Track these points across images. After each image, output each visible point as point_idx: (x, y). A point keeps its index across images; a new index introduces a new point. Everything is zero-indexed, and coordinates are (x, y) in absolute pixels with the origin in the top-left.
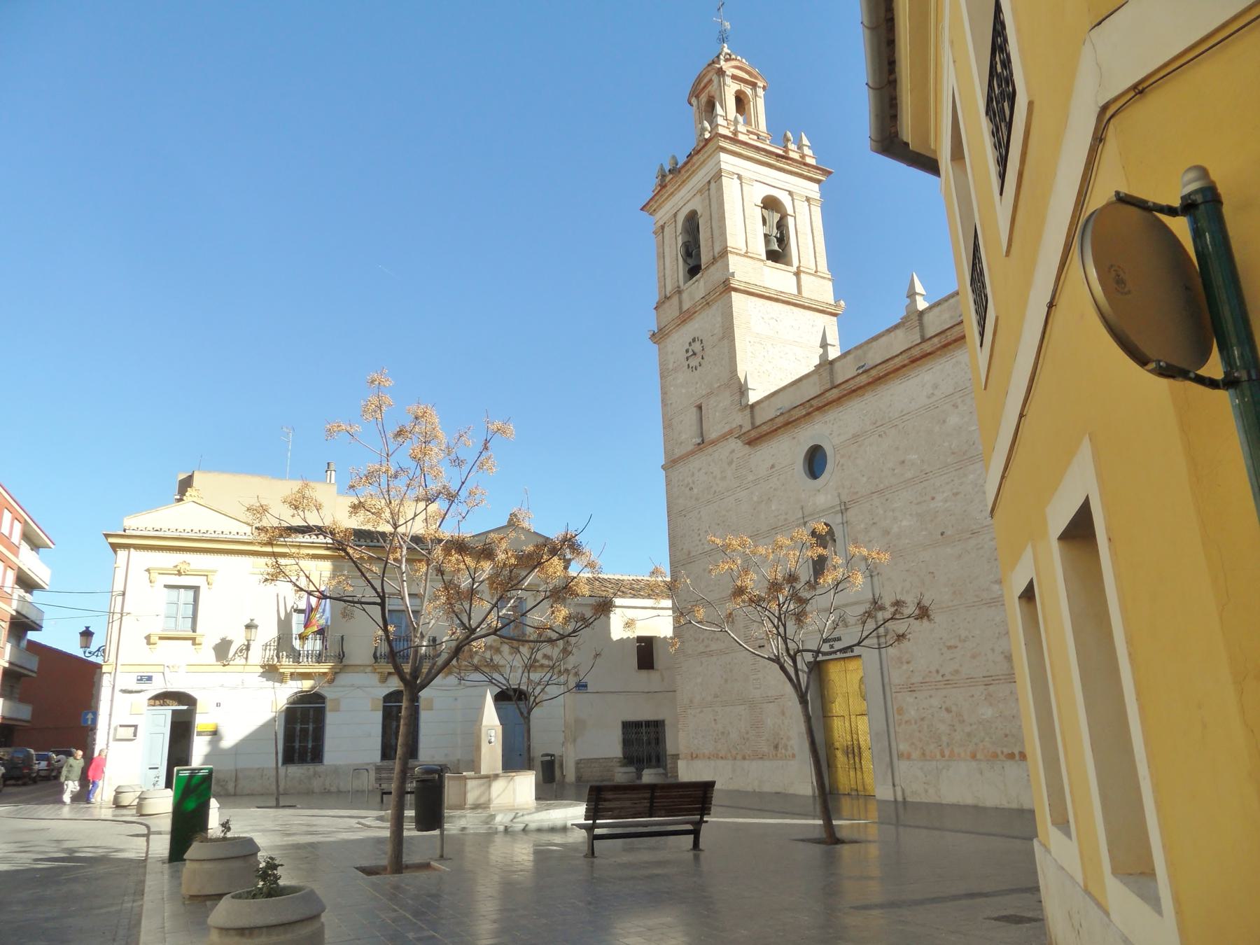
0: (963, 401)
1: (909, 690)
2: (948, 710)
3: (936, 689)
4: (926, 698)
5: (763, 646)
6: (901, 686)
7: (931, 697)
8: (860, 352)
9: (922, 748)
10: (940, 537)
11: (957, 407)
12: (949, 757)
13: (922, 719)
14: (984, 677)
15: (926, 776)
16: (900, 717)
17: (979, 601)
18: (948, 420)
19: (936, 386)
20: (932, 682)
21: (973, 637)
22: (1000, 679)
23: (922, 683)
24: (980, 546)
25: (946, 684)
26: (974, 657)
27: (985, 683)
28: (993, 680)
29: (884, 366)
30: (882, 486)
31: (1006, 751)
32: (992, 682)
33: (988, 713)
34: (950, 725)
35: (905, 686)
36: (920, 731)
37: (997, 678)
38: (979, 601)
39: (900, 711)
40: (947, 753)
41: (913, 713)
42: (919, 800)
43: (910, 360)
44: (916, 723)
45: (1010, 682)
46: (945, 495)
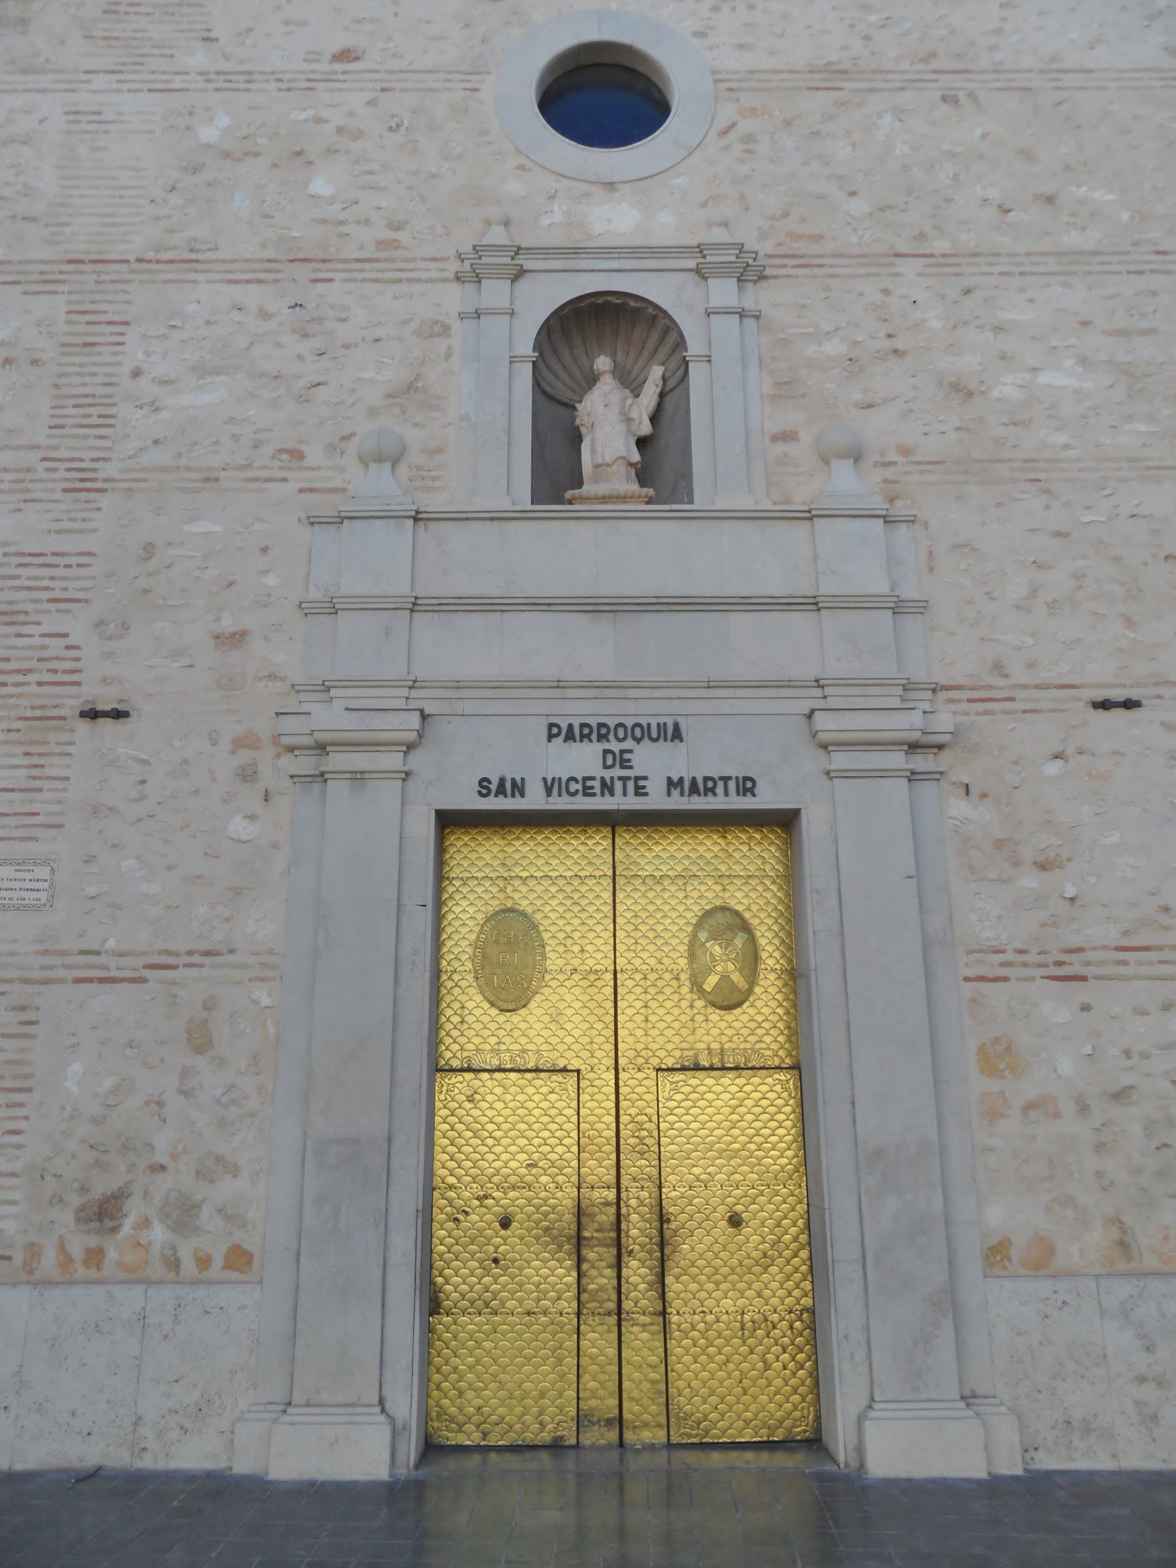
5: (118, 715)
6: (1009, 956)
9: (1116, 1221)
13: (1121, 1095)
16: (994, 1085)
30: (942, 245)
35: (1032, 957)
41: (1066, 1067)
42: (1102, 1463)
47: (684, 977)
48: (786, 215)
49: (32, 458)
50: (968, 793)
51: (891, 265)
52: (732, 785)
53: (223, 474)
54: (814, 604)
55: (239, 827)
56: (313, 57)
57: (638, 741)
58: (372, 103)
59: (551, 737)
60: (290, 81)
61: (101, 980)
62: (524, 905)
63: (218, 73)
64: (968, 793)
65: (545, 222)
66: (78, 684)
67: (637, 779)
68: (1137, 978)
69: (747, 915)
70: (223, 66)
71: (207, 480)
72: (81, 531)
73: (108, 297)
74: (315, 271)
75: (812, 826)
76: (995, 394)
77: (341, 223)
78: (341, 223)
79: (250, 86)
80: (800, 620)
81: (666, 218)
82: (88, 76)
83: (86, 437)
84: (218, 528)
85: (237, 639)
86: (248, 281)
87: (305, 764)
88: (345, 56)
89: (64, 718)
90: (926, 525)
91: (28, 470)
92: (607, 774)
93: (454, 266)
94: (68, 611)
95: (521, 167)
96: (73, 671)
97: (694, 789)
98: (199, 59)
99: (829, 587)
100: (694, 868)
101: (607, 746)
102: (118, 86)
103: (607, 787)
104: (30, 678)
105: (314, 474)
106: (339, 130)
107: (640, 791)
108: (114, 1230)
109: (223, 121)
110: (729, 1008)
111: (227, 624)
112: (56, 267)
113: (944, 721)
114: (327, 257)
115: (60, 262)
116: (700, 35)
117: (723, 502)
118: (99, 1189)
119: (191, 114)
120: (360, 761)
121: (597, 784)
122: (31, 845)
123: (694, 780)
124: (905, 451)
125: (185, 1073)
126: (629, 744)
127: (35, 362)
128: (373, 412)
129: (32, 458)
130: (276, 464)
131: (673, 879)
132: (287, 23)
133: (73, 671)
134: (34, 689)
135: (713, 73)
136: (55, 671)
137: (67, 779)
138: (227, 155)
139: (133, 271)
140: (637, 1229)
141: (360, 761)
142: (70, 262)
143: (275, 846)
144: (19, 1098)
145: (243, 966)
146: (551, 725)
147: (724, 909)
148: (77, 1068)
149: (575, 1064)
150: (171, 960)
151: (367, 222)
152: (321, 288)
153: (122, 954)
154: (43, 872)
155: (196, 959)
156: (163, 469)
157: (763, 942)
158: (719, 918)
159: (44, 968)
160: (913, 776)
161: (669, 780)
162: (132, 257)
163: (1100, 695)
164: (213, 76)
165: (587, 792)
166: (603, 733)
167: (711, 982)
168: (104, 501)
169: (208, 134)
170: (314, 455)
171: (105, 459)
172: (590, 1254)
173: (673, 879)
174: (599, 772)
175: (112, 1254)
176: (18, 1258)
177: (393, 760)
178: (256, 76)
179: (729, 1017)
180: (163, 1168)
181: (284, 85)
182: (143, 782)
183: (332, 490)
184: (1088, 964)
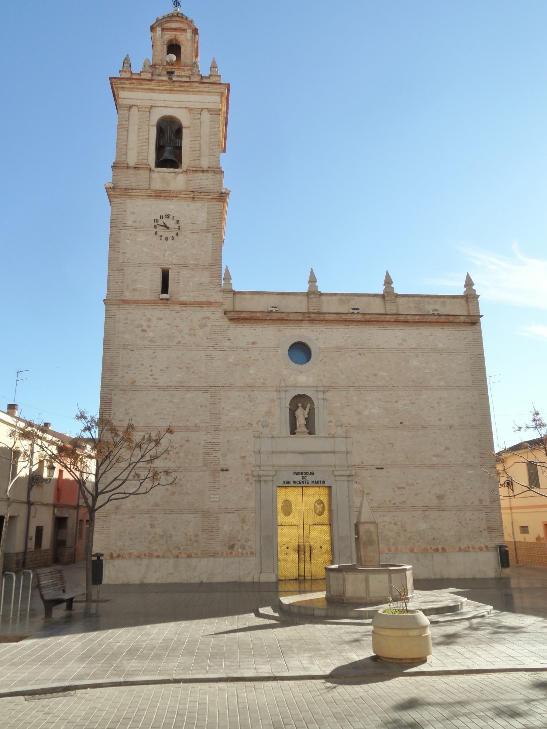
0: (422, 355)
2: (395, 524)
3: (389, 511)
4: (380, 517)
5: (227, 470)
7: (384, 516)
8: (344, 298)
11: (418, 357)
14: (422, 506)
18: (410, 361)
19: (404, 340)
21: (417, 484)
22: (433, 508)
23: (378, 507)
25: (395, 509)
26: (416, 495)
27: (423, 510)
28: (429, 509)
29: (378, 316)
30: (357, 384)
32: (428, 510)
34: (397, 533)
40: (393, 549)
43: (395, 320)
45: (439, 510)
46: (406, 402)
47: (313, 510)
48: (331, 378)
49: (207, 425)
50: (356, 483)
51: (349, 388)
52: (321, 482)
53: (240, 428)
54: (334, 452)
55: (247, 488)
56: (248, 343)
57: (307, 475)
58: (259, 354)
59: (294, 474)
60: (245, 349)
61: (228, 513)
62: (289, 499)
63: (231, 347)
64: (356, 483)
65: (290, 379)
66: (220, 465)
67: (307, 481)
68: (380, 511)
69: (323, 501)
70: (232, 345)
71: (237, 429)
72: (217, 438)
73: (217, 394)
74: (252, 389)
75: (333, 488)
76: (364, 414)
77: (256, 379)
78: (256, 379)
79: (237, 350)
80: (332, 455)
81: (311, 379)
82: (208, 347)
83: (216, 421)
84: (239, 438)
85: (244, 457)
86: (240, 391)
87: (257, 479)
88: (254, 343)
89: (218, 471)
90: (352, 438)
91: (207, 427)
92: (303, 480)
93: (275, 388)
94: (216, 453)
95: (286, 368)
96: (219, 463)
97: (316, 483)
98: (227, 344)
99: (337, 449)
100: (315, 493)
101: (303, 476)
102: (214, 349)
103: (303, 482)
104: (212, 464)
105: (254, 428)
106: (254, 359)
107: (308, 483)
108: (234, 549)
109: (233, 357)
110: (320, 515)
111: (242, 455)
112: (207, 388)
113: (353, 472)
114: (253, 386)
115: (207, 387)
116: (317, 340)
117: (320, 435)
118: (231, 543)
119: (227, 356)
120: (266, 478)
121: (301, 482)
122: (215, 492)
123: (316, 481)
124: (349, 424)
125: (242, 527)
126: (306, 475)
127: (206, 406)
128: (263, 417)
129: (207, 425)
130: (248, 426)
131: (312, 495)
132: (243, 336)
133: (219, 463)
134: (213, 466)
135: (319, 348)
136: (216, 463)
137: (219, 481)
138: (234, 364)
139: (220, 389)
140: (307, 548)
141: (266, 478)
142: (210, 387)
143: (253, 491)
144: (218, 530)
145: (249, 510)
146: (294, 472)
147: (319, 500)
148: (226, 526)
149: (297, 524)
150: (238, 510)
151: (260, 379)
152: (253, 392)
153: (231, 509)
154: (218, 496)
155: (242, 509)
156: (229, 427)
157: (325, 505)
158: (319, 501)
159: (219, 511)
160: (348, 481)
161: (312, 481)
162: (220, 386)
163: (378, 467)
164: (230, 348)
165: (300, 483)
166: (302, 473)
167: (317, 511)
168: (220, 433)
169: (231, 360)
170: (254, 424)
171: (220, 425)
172: (300, 552)
173: (312, 495)
174: (301, 479)
175: (234, 553)
176: (220, 553)
177: (270, 478)
178: (238, 348)
179: (320, 517)
180: (240, 540)
181: (244, 350)
182: (231, 481)
183: (257, 431)
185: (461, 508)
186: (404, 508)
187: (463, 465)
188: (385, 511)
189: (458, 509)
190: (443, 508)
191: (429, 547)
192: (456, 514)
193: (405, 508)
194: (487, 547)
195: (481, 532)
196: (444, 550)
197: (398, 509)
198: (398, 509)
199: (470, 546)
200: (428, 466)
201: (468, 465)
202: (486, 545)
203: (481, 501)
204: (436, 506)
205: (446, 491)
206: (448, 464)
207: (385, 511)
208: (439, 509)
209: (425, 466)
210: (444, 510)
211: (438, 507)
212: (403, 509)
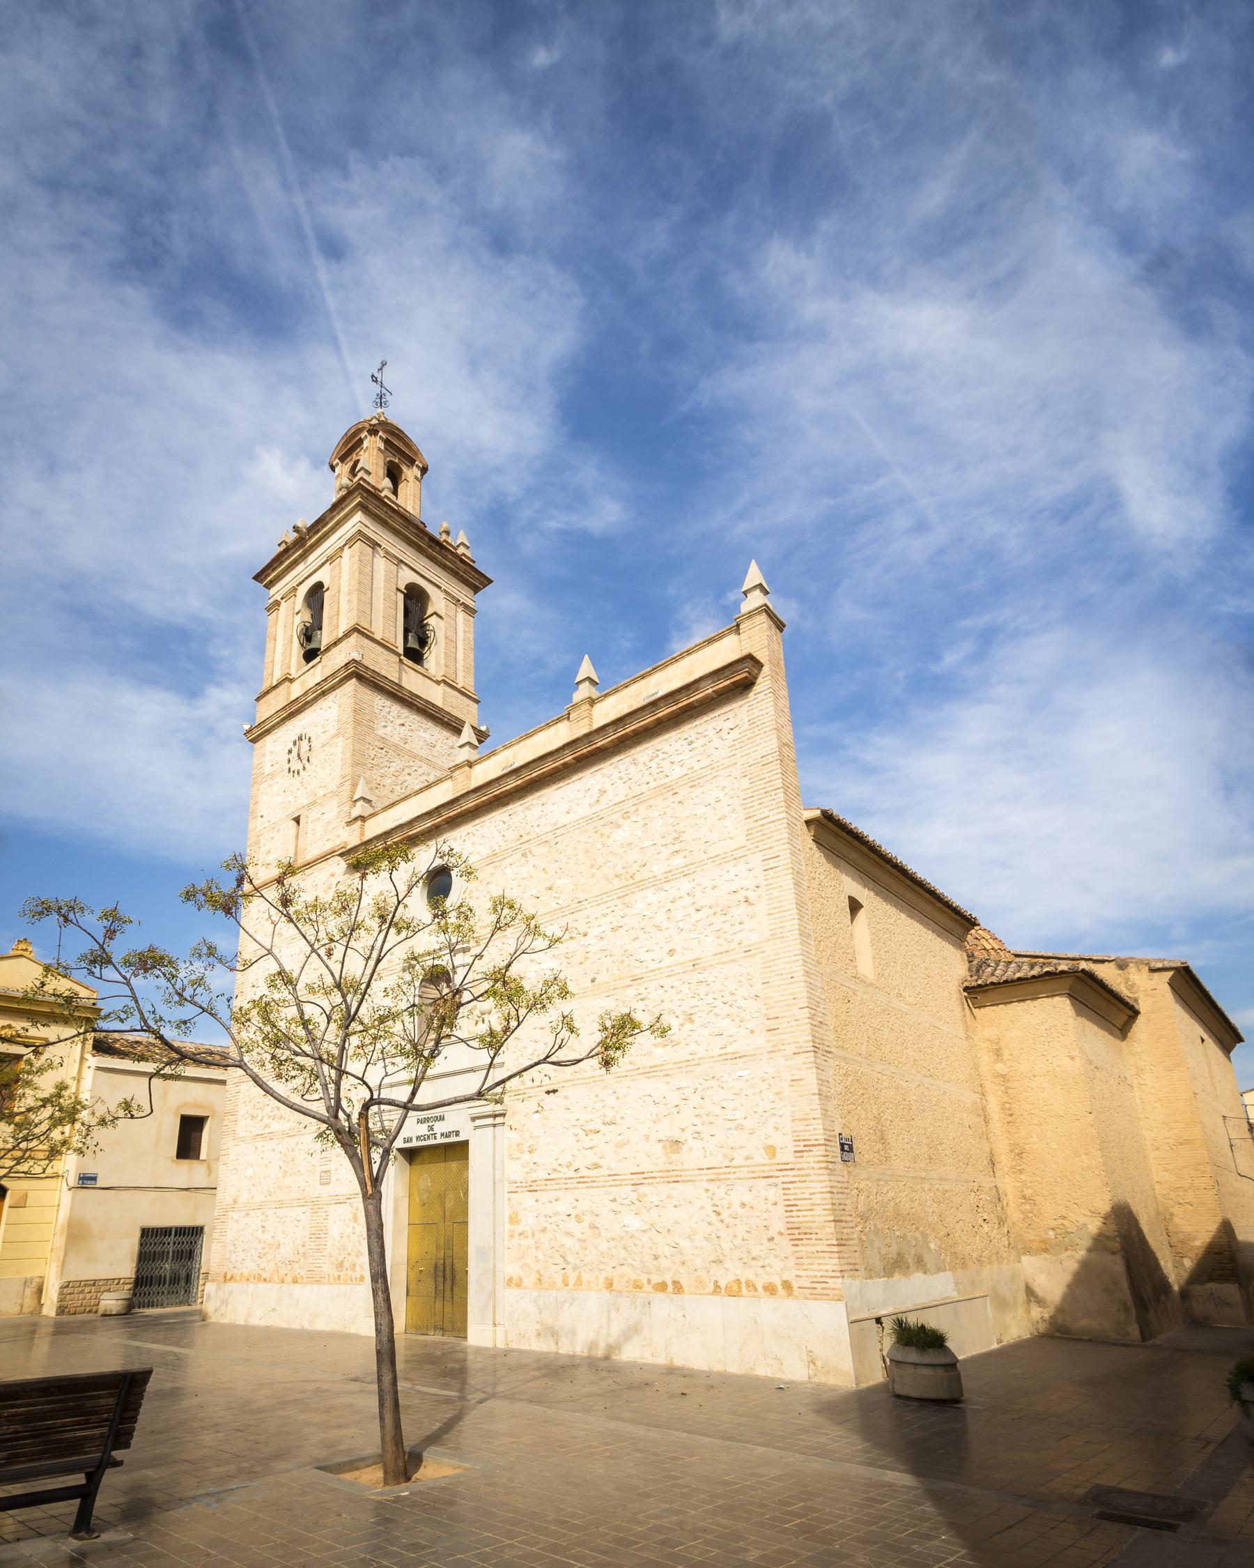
1: (530, 1189)
2: (579, 1219)
3: (566, 1189)
10: (589, 984)
12: (574, 1285)
15: (540, 1313)
16: (512, 1227)
17: (635, 1070)
20: (561, 1179)
21: (622, 1118)
23: (546, 1180)
24: (641, 997)
25: (578, 1183)
26: (621, 1145)
28: (645, 1178)
31: (656, 1279)
32: (643, 1181)
33: (635, 1224)
36: (537, 1248)
37: (651, 1175)
38: (635, 1070)
39: (514, 1219)
40: (572, 1281)
44: (533, 1235)
45: (669, 1182)
184: (537, 1186)
185: (719, 1174)
186: (593, 1179)
187: (725, 1057)
188: (560, 1189)
189: (712, 1177)
190: (677, 1176)
191: (644, 1279)
192: (707, 1191)
193: (597, 1179)
194: (787, 1285)
195: (771, 1239)
196: (678, 1287)
197: (584, 1182)
198: (584, 1182)
199: (743, 1281)
200: (644, 1071)
201: (738, 1055)
202: (785, 1278)
203: (771, 1151)
204: (662, 1171)
205: (683, 1130)
206: (688, 1061)
207: (560, 1189)
208: (669, 1179)
209: (639, 1072)
210: (678, 1182)
211: (664, 1174)
212: (592, 1182)
